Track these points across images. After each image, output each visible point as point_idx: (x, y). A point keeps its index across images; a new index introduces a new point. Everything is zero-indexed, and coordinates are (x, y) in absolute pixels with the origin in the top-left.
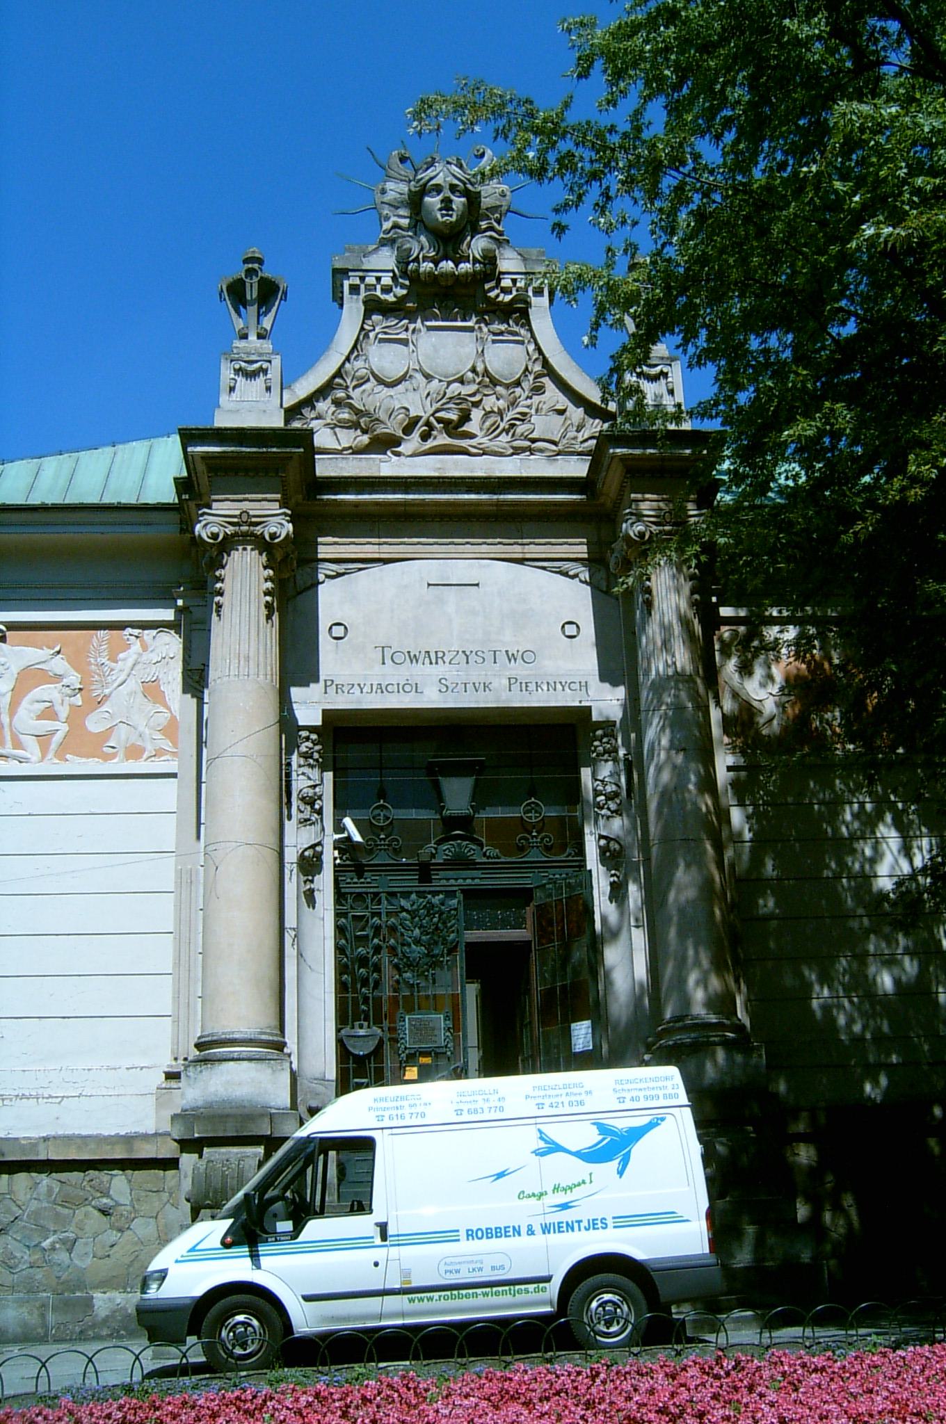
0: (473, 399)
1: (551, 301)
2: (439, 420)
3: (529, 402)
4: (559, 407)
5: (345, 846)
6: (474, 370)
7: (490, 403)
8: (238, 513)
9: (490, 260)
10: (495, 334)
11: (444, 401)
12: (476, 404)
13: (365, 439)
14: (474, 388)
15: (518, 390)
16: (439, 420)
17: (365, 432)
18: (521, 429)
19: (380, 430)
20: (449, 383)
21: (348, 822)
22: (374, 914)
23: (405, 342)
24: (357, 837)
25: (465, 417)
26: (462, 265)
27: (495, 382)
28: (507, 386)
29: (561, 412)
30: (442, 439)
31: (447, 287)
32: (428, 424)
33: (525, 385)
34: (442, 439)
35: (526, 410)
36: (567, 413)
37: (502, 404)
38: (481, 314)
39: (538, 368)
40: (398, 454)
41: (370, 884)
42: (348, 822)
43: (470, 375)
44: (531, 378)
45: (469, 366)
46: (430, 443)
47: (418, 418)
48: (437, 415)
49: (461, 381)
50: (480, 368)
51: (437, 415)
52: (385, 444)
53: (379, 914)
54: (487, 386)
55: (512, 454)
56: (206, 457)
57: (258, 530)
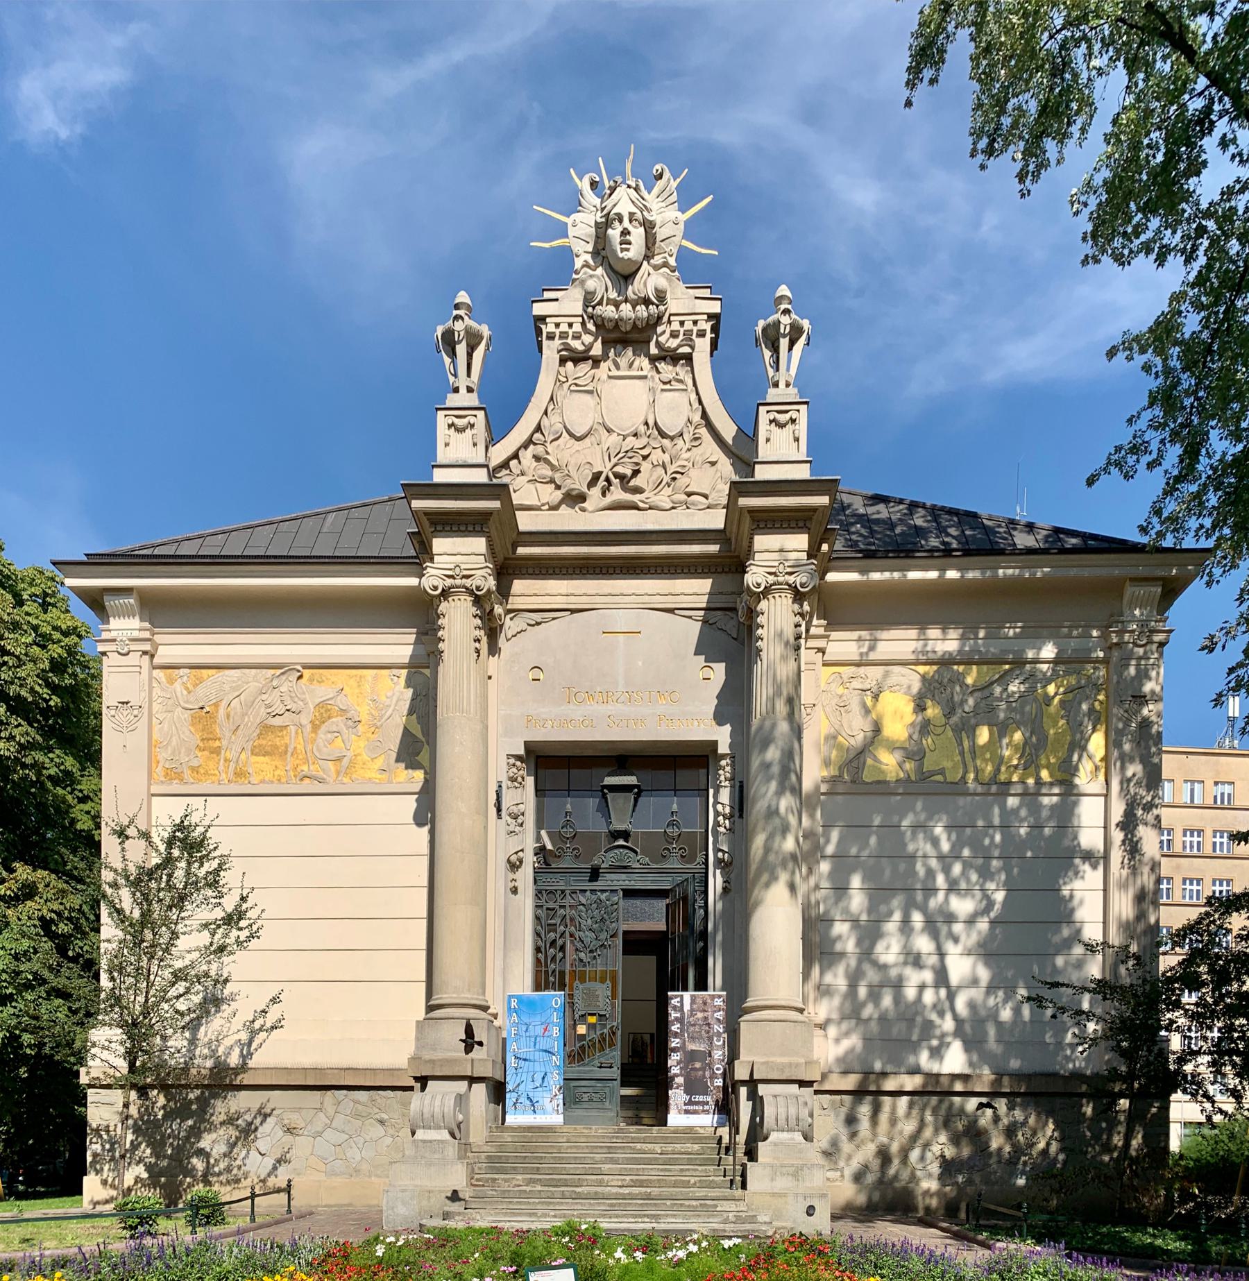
0: (645, 452)
1: (714, 345)
2: (617, 475)
3: (689, 454)
4: (713, 459)
5: (541, 851)
6: (646, 424)
7: (657, 456)
8: (452, 566)
9: (661, 297)
10: (665, 383)
11: (621, 455)
12: (645, 458)
13: (558, 495)
14: (644, 441)
15: (680, 442)
16: (617, 475)
17: (558, 487)
18: (682, 481)
19: (568, 485)
20: (625, 438)
21: (543, 833)
22: (561, 907)
23: (590, 392)
24: (549, 847)
25: (636, 473)
26: (638, 308)
27: (663, 435)
28: (672, 438)
29: (713, 464)
30: (617, 494)
31: (627, 333)
32: (607, 479)
33: (686, 436)
34: (617, 494)
35: (685, 463)
36: (718, 465)
37: (666, 458)
38: (653, 360)
39: (697, 418)
40: (583, 510)
41: (560, 883)
42: (543, 833)
43: (642, 429)
44: (691, 429)
45: (642, 419)
46: (610, 499)
47: (601, 473)
48: (615, 469)
49: (635, 435)
50: (651, 423)
51: (615, 469)
52: (575, 499)
53: (563, 907)
54: (655, 439)
55: (673, 508)
56: (428, 514)
57: (468, 582)
